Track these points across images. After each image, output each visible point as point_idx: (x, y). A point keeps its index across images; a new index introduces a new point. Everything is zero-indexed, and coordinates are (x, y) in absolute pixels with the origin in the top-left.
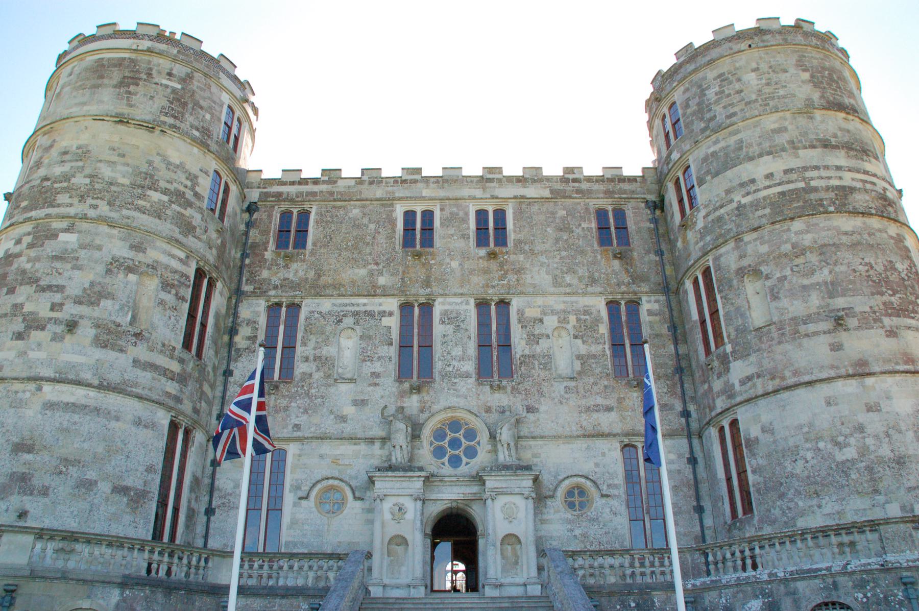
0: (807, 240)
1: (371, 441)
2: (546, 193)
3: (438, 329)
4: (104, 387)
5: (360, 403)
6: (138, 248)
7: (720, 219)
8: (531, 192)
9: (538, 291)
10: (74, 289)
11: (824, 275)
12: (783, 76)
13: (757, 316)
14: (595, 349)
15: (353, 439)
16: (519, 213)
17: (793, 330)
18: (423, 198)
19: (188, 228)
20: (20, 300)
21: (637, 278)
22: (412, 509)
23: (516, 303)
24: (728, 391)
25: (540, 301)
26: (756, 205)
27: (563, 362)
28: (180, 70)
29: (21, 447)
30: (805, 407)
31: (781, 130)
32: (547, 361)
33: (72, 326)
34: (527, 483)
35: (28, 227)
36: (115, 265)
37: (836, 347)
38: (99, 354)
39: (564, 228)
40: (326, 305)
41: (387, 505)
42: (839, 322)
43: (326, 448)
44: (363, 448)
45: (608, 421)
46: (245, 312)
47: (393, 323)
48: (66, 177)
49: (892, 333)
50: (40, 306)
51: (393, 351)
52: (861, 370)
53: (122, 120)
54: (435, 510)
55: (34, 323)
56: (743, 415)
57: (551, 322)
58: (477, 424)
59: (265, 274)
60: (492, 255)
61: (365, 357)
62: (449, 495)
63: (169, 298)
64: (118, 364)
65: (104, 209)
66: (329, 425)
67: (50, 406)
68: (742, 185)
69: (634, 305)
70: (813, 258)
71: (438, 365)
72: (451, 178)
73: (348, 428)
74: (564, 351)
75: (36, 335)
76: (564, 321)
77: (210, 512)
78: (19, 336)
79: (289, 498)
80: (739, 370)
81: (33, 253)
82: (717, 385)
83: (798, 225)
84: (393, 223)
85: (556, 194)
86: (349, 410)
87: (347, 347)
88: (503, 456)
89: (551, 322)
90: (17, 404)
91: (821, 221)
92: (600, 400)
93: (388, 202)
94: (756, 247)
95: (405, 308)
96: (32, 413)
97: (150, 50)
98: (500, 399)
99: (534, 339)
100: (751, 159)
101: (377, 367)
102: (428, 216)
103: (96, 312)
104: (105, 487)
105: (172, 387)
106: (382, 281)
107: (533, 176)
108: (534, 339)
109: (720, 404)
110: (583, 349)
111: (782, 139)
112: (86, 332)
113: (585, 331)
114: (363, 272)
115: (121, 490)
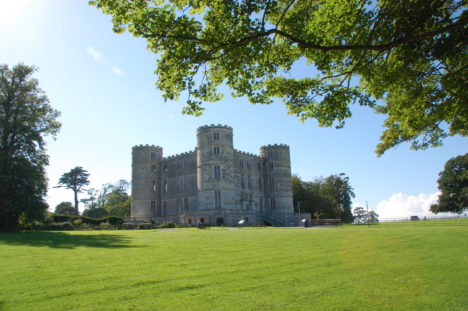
3: (245, 180)
8: (252, 158)
13: (279, 187)
24: (274, 195)
26: (282, 173)
35: (226, 165)
39: (255, 166)
45: (259, 195)
47: (240, 178)
50: (230, 179)
56: (276, 198)
58: (248, 194)
75: (231, 184)
80: (276, 193)
82: (272, 194)
85: (255, 160)
98: (250, 191)
99: (253, 183)
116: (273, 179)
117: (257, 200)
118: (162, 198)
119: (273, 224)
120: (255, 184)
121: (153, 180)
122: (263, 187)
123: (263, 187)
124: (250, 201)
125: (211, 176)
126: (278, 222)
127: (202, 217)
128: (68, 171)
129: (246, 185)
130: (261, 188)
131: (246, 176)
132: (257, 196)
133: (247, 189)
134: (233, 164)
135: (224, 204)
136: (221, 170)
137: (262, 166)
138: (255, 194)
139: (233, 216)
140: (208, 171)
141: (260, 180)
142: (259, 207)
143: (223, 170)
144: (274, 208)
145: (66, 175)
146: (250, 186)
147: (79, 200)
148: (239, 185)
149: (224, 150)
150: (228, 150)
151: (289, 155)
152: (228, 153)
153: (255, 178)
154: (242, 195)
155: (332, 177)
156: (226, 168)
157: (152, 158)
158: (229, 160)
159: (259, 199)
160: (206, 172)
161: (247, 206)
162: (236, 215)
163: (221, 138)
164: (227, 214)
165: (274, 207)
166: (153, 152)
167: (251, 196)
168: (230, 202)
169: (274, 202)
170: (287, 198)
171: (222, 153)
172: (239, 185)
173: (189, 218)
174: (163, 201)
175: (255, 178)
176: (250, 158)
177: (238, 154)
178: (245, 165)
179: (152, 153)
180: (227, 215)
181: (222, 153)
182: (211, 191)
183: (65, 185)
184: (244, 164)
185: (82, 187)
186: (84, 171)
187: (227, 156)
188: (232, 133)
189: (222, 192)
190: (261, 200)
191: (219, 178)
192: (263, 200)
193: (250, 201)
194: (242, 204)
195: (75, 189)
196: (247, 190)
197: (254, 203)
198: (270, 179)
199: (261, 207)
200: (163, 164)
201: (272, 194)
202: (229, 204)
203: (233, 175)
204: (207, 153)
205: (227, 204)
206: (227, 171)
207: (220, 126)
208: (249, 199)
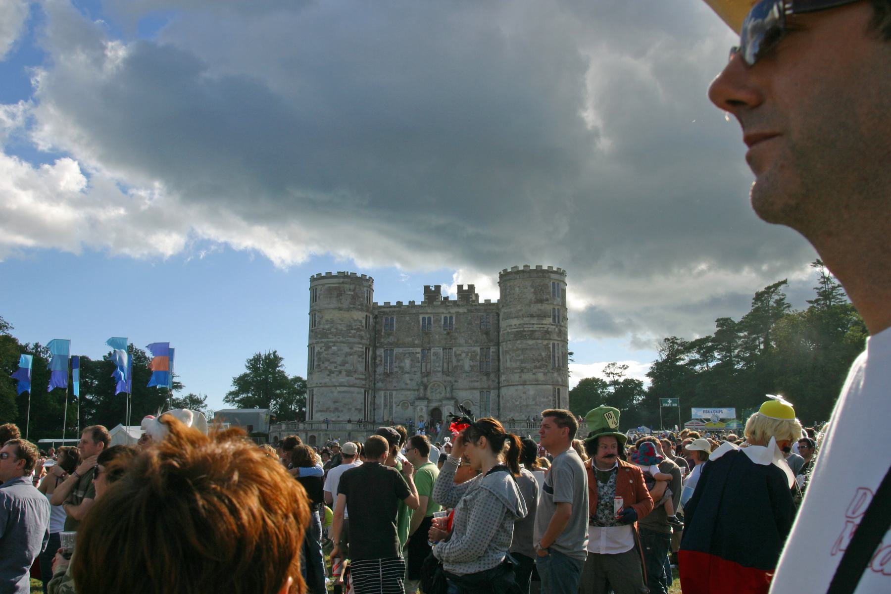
1: (414, 390)
2: (466, 311)
4: (350, 386)
5: (411, 380)
6: (351, 348)
9: (461, 346)
10: (338, 363)
11: (521, 357)
14: (475, 364)
15: (409, 390)
16: (457, 317)
18: (427, 313)
19: (361, 337)
22: (425, 409)
25: (461, 348)
26: (511, 333)
27: (467, 367)
28: (352, 287)
29: (335, 402)
31: (521, 310)
32: (462, 367)
33: (340, 372)
34: (453, 402)
36: (348, 354)
37: (520, 377)
38: (347, 378)
39: (470, 323)
40: (401, 350)
41: (418, 408)
42: (522, 371)
43: (403, 392)
44: (412, 392)
45: (477, 385)
46: (378, 353)
47: (419, 356)
49: (534, 374)
50: (332, 367)
52: (524, 384)
53: (340, 309)
54: (431, 408)
55: (331, 372)
57: (464, 355)
59: (382, 340)
61: (412, 366)
62: (434, 405)
63: (360, 359)
64: (352, 380)
65: (341, 339)
66: (403, 386)
67: (339, 392)
70: (520, 352)
73: (408, 387)
74: (467, 364)
76: (467, 355)
77: (374, 409)
79: (394, 406)
83: (519, 342)
84: (419, 321)
86: (409, 382)
87: (407, 363)
88: (448, 395)
89: (464, 355)
90: (332, 392)
91: (525, 342)
93: (417, 314)
96: (335, 394)
97: (343, 283)
101: (416, 369)
102: (429, 318)
103: (344, 368)
104: (353, 409)
105: (364, 382)
106: (416, 342)
108: (458, 361)
110: (472, 363)
111: (520, 314)
112: (344, 373)
113: (473, 359)
114: (410, 339)
115: (356, 409)
133: (439, 375)
135: (317, 412)
148: (413, 370)
168: (328, 409)
170: (520, 387)
171: (319, 323)
175: (465, 349)
187: (327, 327)
205: (321, 411)
206: (324, 355)
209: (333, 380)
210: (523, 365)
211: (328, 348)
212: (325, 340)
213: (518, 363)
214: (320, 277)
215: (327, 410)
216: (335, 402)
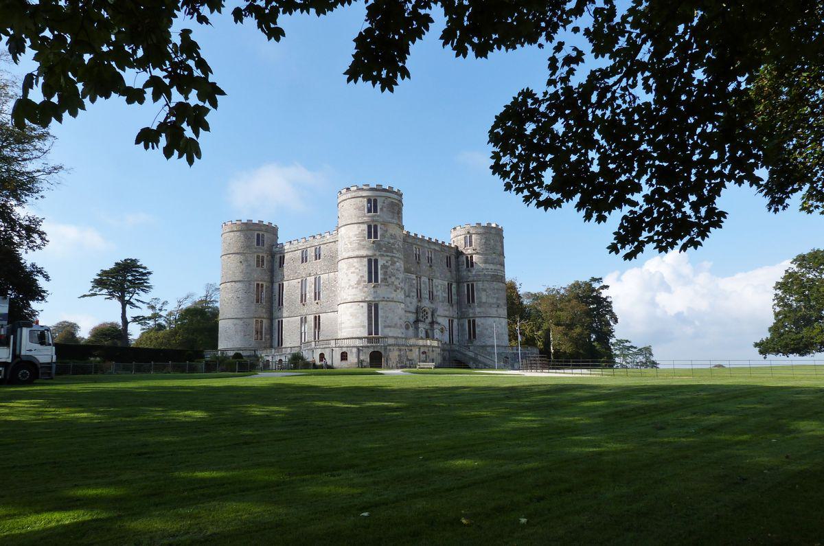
0: (496, 287)
1: (413, 313)
3: (423, 286)
5: (411, 303)
7: (479, 275)
8: (437, 248)
9: (438, 278)
11: (497, 295)
12: (497, 244)
15: (409, 312)
17: (491, 305)
20: (393, 280)
21: (453, 278)
23: (434, 280)
26: (488, 275)
30: (490, 321)
35: (389, 258)
37: (497, 311)
47: (414, 282)
48: (394, 244)
50: (396, 283)
51: (415, 290)
56: (477, 320)
57: (439, 286)
58: (428, 310)
60: (431, 266)
68: (486, 269)
69: (451, 285)
71: (423, 295)
72: (422, 239)
75: (398, 291)
78: (395, 291)
80: (478, 310)
81: (392, 267)
82: (471, 311)
83: (495, 283)
92: (445, 308)
94: (486, 285)
95: (417, 277)
100: (489, 264)
107: (436, 243)
109: (471, 315)
110: (444, 295)
111: (495, 261)
116: (473, 285)
117: (444, 322)
118: (275, 314)
119: (471, 364)
120: (441, 293)
121: (260, 283)
122: (455, 297)
123: (455, 297)
124: (432, 323)
125: (363, 276)
126: (480, 362)
127: (344, 350)
128: (109, 265)
129: (425, 294)
130: (450, 300)
131: (425, 279)
132: (444, 314)
133: (427, 301)
134: (402, 257)
135: (385, 327)
136: (379, 267)
137: (453, 259)
138: (440, 311)
139: (400, 350)
140: (357, 268)
141: (450, 286)
142: (447, 334)
143: (384, 267)
144: (474, 337)
145: (104, 273)
146: (432, 297)
147: (129, 319)
148: (412, 294)
149: (386, 231)
150: (393, 230)
151: (502, 243)
152: (393, 237)
153: (440, 285)
154: (417, 313)
155: (577, 285)
156: (390, 262)
157: (258, 244)
158: (395, 249)
159: (447, 320)
160: (353, 270)
161: (426, 332)
162: (403, 348)
163: (381, 209)
164: (390, 345)
165: (473, 334)
166: (261, 233)
167: (432, 315)
168: (396, 324)
169: (472, 325)
170: (498, 319)
172: (412, 294)
173: (319, 351)
174: (277, 321)
176: (433, 247)
177: (411, 241)
178: (424, 261)
179: (258, 235)
180: (388, 348)
181: (382, 235)
182: (361, 304)
183: (105, 291)
184: (421, 257)
185: (135, 296)
186: (139, 267)
187: (392, 241)
188: (401, 201)
189: (380, 306)
190: (451, 322)
191: (376, 280)
192: (455, 322)
193: (432, 323)
194: (417, 328)
195: (121, 299)
196: (426, 304)
197: (440, 327)
198: (468, 285)
199: (451, 334)
200: (278, 256)
201: (471, 311)
202: (394, 327)
203: (401, 276)
204: (356, 235)
205: (389, 327)
207: (380, 188)
208: (429, 320)
209: (399, 296)
210: (499, 302)
211: (393, 263)
212: (391, 254)
213: (495, 300)
214: (378, 189)
215: (395, 326)
216: (400, 319)
